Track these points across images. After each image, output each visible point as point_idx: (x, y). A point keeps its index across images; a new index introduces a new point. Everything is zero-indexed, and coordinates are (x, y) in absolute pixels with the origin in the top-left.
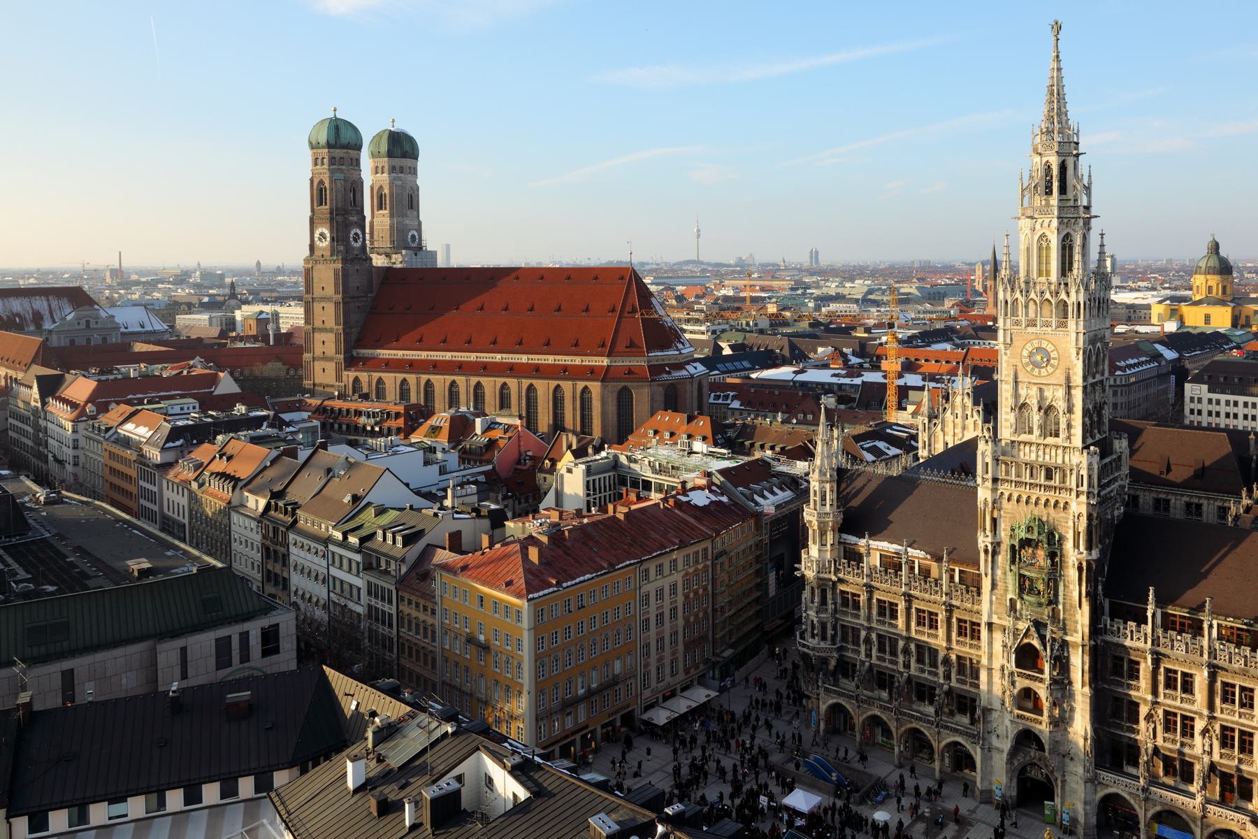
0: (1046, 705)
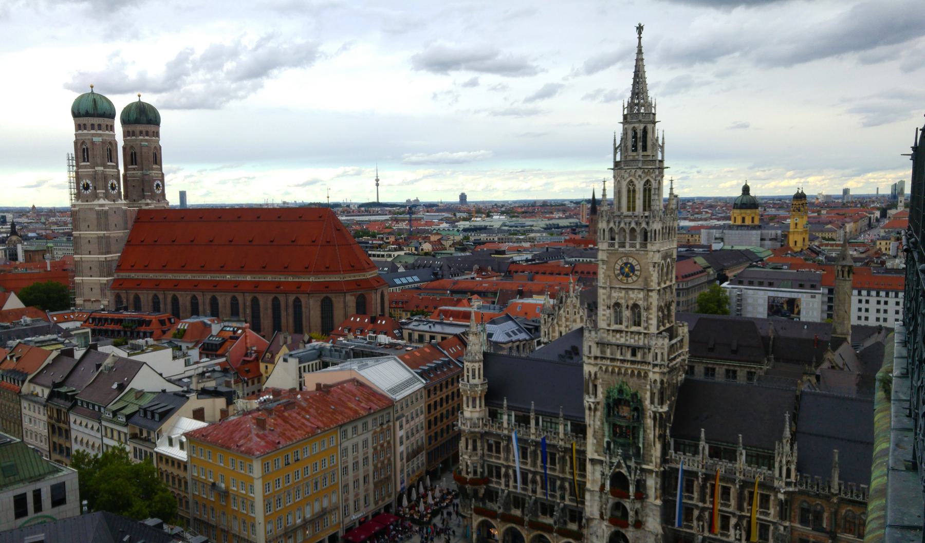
0: (631, 513)
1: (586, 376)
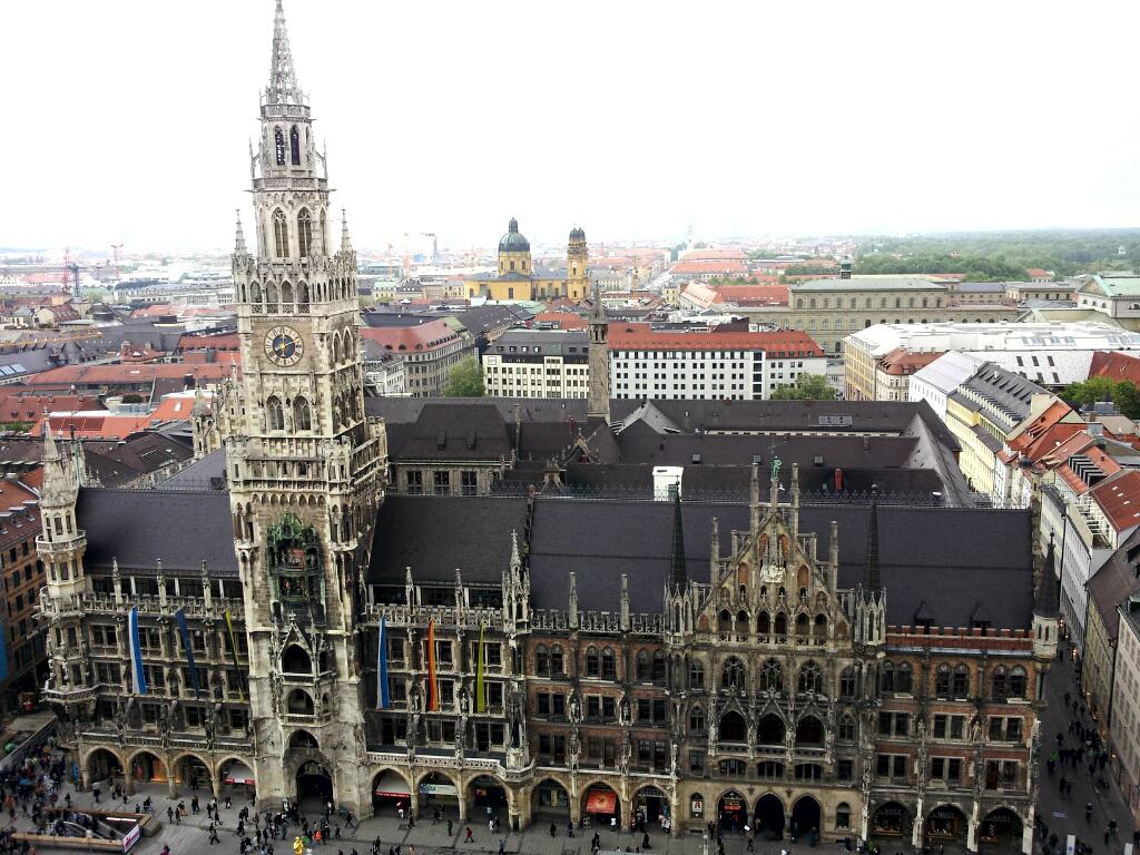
0: (316, 702)
1: (235, 511)
